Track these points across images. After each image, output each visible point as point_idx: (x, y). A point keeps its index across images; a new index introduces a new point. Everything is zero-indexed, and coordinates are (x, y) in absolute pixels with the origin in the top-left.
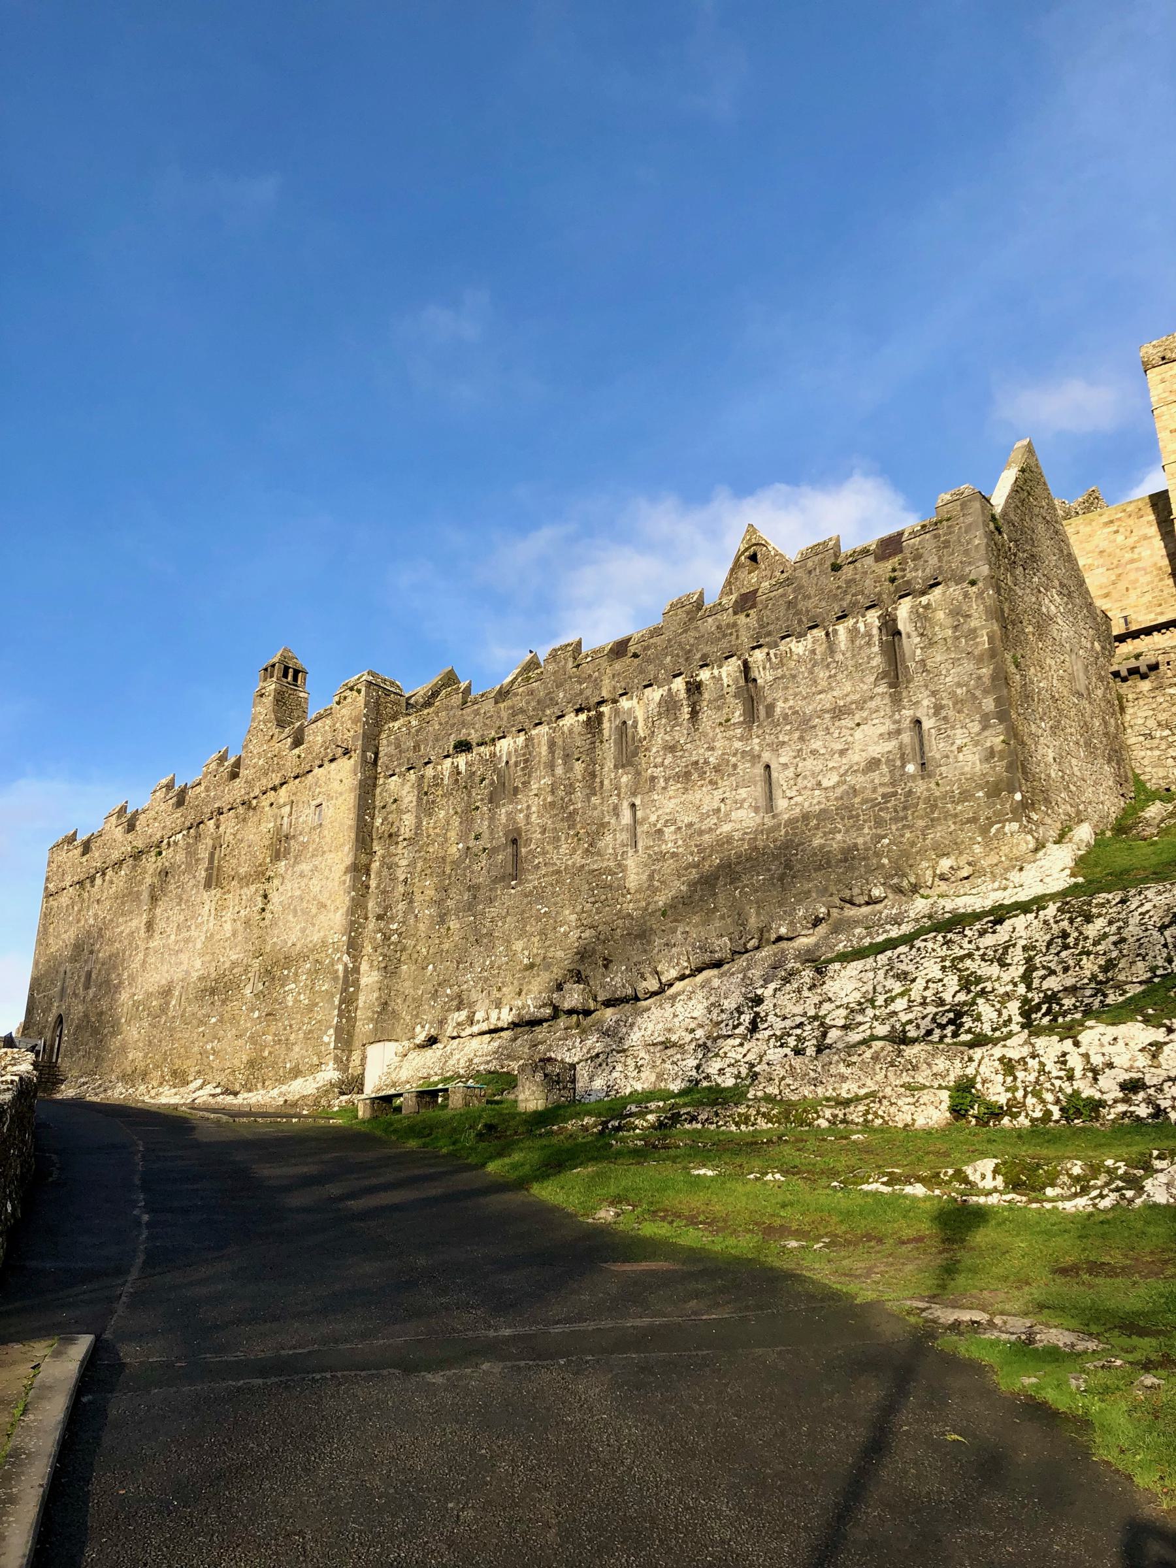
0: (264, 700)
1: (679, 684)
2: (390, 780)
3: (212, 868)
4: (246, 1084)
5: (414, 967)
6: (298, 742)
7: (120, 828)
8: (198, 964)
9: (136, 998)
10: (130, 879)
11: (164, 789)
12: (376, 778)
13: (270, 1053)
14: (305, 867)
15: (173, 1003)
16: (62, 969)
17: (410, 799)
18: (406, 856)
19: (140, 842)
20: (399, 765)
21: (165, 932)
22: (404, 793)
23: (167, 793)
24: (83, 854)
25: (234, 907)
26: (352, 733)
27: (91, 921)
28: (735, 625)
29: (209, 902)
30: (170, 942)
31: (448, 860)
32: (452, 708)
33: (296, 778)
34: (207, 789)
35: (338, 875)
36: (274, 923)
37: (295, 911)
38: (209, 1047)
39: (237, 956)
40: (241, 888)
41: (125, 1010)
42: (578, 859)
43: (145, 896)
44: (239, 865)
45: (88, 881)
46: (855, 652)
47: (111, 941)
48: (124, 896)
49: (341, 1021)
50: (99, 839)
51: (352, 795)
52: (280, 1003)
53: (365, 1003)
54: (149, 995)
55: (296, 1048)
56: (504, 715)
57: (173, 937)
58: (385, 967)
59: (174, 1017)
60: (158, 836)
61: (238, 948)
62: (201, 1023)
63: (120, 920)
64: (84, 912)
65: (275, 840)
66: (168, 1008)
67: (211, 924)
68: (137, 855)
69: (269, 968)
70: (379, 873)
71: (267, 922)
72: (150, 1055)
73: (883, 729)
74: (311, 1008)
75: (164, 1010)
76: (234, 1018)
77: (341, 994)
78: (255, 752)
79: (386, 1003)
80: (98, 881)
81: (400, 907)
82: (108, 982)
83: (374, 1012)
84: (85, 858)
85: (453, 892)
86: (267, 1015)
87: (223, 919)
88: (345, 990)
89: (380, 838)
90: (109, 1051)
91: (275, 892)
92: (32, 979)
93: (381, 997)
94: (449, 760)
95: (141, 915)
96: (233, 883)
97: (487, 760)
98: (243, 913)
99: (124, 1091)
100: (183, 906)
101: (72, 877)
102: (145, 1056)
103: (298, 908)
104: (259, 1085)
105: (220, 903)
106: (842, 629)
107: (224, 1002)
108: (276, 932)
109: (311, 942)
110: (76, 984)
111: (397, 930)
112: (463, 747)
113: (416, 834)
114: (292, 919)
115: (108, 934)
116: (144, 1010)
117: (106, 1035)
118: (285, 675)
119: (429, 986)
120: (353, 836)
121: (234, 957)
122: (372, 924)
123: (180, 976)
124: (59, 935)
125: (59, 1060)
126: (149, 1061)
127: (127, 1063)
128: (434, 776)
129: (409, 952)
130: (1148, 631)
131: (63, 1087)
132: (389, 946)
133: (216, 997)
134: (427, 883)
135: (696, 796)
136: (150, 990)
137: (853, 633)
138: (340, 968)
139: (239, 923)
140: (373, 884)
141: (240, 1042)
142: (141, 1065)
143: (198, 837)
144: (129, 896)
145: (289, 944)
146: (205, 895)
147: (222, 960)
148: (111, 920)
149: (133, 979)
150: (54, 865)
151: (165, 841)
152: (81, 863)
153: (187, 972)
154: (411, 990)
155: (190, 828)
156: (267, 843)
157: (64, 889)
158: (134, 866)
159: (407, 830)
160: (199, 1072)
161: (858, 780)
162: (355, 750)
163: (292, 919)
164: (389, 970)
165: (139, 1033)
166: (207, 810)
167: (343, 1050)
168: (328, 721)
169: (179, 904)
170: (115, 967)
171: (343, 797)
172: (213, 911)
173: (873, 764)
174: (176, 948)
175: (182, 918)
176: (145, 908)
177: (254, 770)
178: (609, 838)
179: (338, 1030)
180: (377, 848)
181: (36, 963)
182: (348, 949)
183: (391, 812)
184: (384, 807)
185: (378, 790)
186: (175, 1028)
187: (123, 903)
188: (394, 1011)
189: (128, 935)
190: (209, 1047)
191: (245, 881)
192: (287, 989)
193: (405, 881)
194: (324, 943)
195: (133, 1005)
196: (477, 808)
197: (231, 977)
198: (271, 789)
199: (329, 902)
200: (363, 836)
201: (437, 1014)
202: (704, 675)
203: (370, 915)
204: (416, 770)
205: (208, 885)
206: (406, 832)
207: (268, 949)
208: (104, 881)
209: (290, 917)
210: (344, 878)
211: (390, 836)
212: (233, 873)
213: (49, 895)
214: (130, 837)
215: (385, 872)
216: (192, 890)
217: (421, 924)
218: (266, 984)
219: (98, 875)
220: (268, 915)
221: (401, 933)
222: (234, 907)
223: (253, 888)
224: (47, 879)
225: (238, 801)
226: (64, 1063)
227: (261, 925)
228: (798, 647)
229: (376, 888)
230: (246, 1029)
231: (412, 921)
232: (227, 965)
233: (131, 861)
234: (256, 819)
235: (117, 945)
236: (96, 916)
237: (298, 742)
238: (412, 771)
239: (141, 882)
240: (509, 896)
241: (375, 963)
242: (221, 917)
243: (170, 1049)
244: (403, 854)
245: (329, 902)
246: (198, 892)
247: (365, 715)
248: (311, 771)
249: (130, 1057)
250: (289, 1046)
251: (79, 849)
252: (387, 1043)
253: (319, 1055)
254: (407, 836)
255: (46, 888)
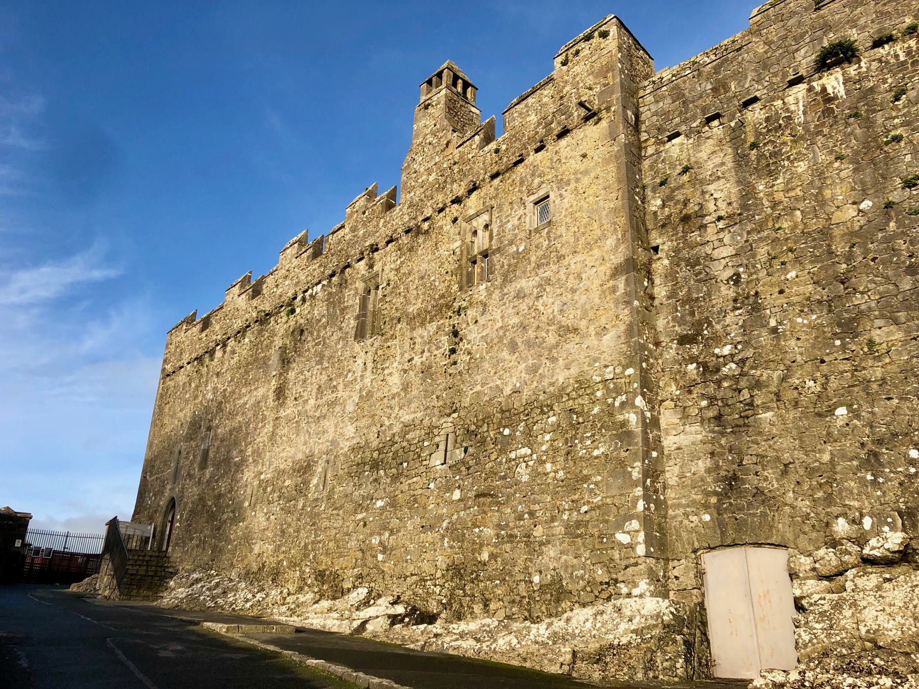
0: (431, 110)
2: (668, 145)
3: (365, 315)
4: (450, 603)
5: (791, 415)
7: (243, 296)
8: (350, 430)
9: (262, 477)
10: (255, 345)
11: (296, 245)
12: (640, 148)
13: (493, 556)
14: (525, 284)
15: (315, 481)
16: (176, 450)
17: (717, 160)
18: (727, 240)
19: (268, 305)
20: (684, 121)
21: (301, 396)
22: (703, 155)
23: (299, 249)
24: (203, 330)
25: (402, 355)
26: (598, 89)
27: (210, 396)
29: (362, 354)
30: (308, 407)
31: (837, 232)
32: (793, 13)
33: (493, 177)
34: (354, 229)
35: (597, 282)
36: (474, 364)
37: (513, 347)
38: (375, 541)
39: (413, 416)
40: (413, 329)
41: (249, 491)
43: (274, 360)
44: (408, 302)
45: (207, 355)
47: (232, 415)
48: (247, 365)
49: (648, 509)
50: (220, 311)
51: (612, 167)
52: (504, 478)
53: (681, 476)
54: (280, 473)
55: (551, 552)
57: (312, 402)
58: (719, 418)
59: (317, 500)
60: (290, 294)
61: (413, 405)
62: (359, 507)
63: (244, 390)
64: (202, 388)
65: (464, 261)
66: (308, 488)
67: (367, 381)
68: (264, 319)
69: (473, 427)
70: (671, 276)
71: (460, 367)
72: (283, 549)
74: (575, 482)
75: (301, 490)
76: (415, 501)
77: (643, 462)
78: (422, 170)
79: (735, 477)
80: (219, 354)
81: (728, 320)
82: (227, 460)
83: (707, 494)
84: (204, 334)
85: (863, 282)
86: (477, 496)
87: (386, 372)
88: (647, 455)
89: (663, 226)
90: (228, 541)
91: (472, 326)
92: (146, 461)
93: (718, 467)
94: (803, 87)
95: (269, 382)
96: (399, 326)
97: (903, 63)
98: (417, 360)
99: (250, 596)
100: (326, 364)
101: (190, 354)
102: (277, 550)
103: (519, 341)
104: (478, 608)
105: (380, 352)
107: (395, 478)
108: (479, 378)
109: (552, 384)
110: (192, 463)
111: (732, 355)
113: (744, 207)
114: (508, 357)
115: (228, 407)
116: (273, 491)
117: (225, 521)
118: (455, 84)
119: (849, 445)
120: (622, 220)
121: (407, 418)
122: (671, 352)
123: (324, 448)
124: (175, 414)
125: (170, 549)
126: (282, 557)
127: (251, 557)
128: (767, 120)
129: (774, 389)
131: (172, 583)
132: (719, 383)
133: (382, 472)
134: (792, 275)
136: (282, 467)
138: (632, 418)
139: (411, 373)
140: (661, 291)
141: (430, 536)
142: (271, 561)
143: (343, 284)
144: (257, 362)
145: (507, 391)
146: (357, 347)
147: (387, 423)
148: (233, 392)
149: (259, 455)
150: (172, 347)
151: (299, 298)
152: (200, 339)
153: (334, 442)
154: (801, 455)
155: (332, 275)
156: (451, 268)
157: (182, 367)
158: (260, 332)
159: (722, 205)
160: (360, 576)
162: (608, 109)
163: (508, 357)
165: (268, 519)
166: (355, 252)
167: (658, 559)
168: (548, 91)
169: (320, 362)
170: (236, 443)
171: (592, 175)
172: (370, 365)
174: (317, 414)
175: (324, 378)
176: (274, 373)
177: (422, 190)
180: (659, 241)
181: (150, 445)
182: (642, 387)
183: (682, 186)
184: (662, 184)
185: (646, 164)
186: (318, 515)
187: (247, 372)
188: (759, 492)
189: (253, 405)
190: (375, 541)
191: (421, 319)
192: (513, 455)
193: (736, 279)
194: (583, 384)
195: (260, 486)
196: (897, 139)
197: (405, 444)
198: (453, 202)
199: (583, 323)
200: (637, 222)
201: (890, 496)
203: (664, 339)
204: (724, 120)
205: (360, 334)
207: (466, 402)
208: (225, 352)
209: (505, 354)
210: (611, 283)
211: (686, 219)
212: (398, 315)
213: (166, 375)
214: (255, 302)
215: (684, 272)
216: (337, 343)
217: (793, 342)
218: (471, 450)
219: (219, 347)
220: (462, 358)
221: (743, 361)
222: (402, 355)
223: (432, 327)
224: (165, 361)
225: (400, 230)
226: (175, 553)
227: (450, 371)
229: (669, 298)
230: (440, 518)
231: (765, 338)
232: (396, 429)
233: (256, 327)
234: (429, 243)
235: (239, 418)
236: (215, 389)
238: (716, 123)
239: (268, 347)
241: (694, 411)
242: (383, 369)
243: (313, 542)
244: (721, 240)
245: (583, 323)
246: (345, 345)
247: (620, 62)
248: (521, 161)
249: (256, 550)
250: (533, 547)
251: (197, 327)
252: (752, 551)
253: (609, 565)
254: (723, 213)
255: (164, 369)
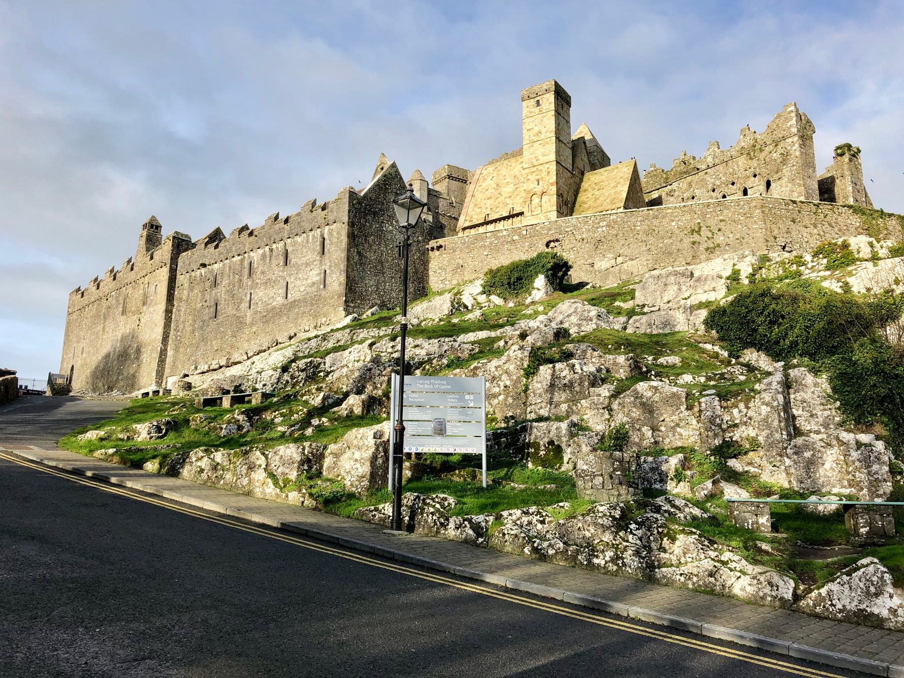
1: (267, 248)
6: (152, 258)
10: (97, 309)
14: (151, 309)
28: (283, 228)
42: (234, 312)
43: (102, 317)
46: (314, 243)
56: (217, 254)
73: (317, 272)
80: (87, 310)
106: (311, 234)
112: (204, 265)
130: (495, 221)
135: (268, 291)
137: (314, 235)
144: (97, 316)
161: (309, 289)
164: (177, 350)
173: (314, 283)
178: (243, 305)
179: (158, 372)
202: (274, 246)
206: (184, 298)
214: (98, 291)
228: (299, 239)
237: (152, 258)
240: (213, 324)
